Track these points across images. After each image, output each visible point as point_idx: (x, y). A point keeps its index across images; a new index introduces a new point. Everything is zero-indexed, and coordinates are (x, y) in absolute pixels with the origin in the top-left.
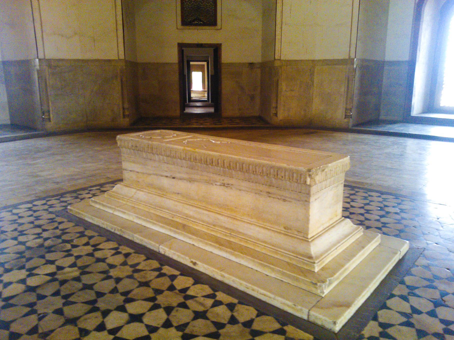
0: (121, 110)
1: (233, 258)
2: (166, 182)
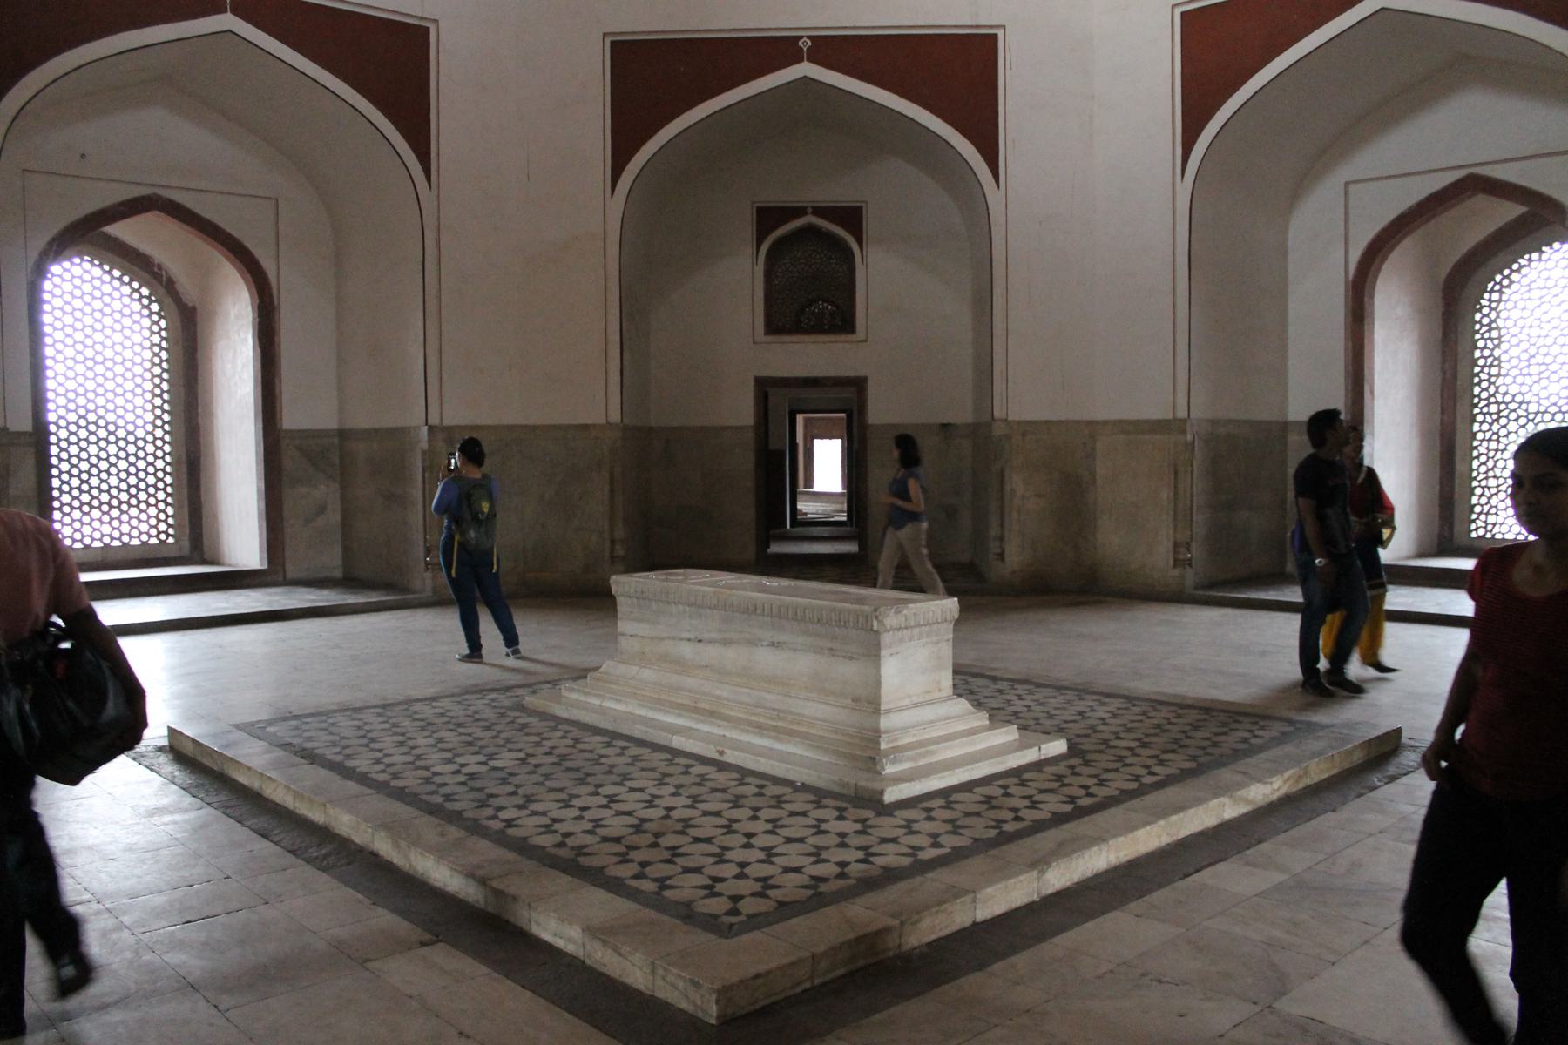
0: (608, 544)
1: (778, 746)
2: (687, 650)
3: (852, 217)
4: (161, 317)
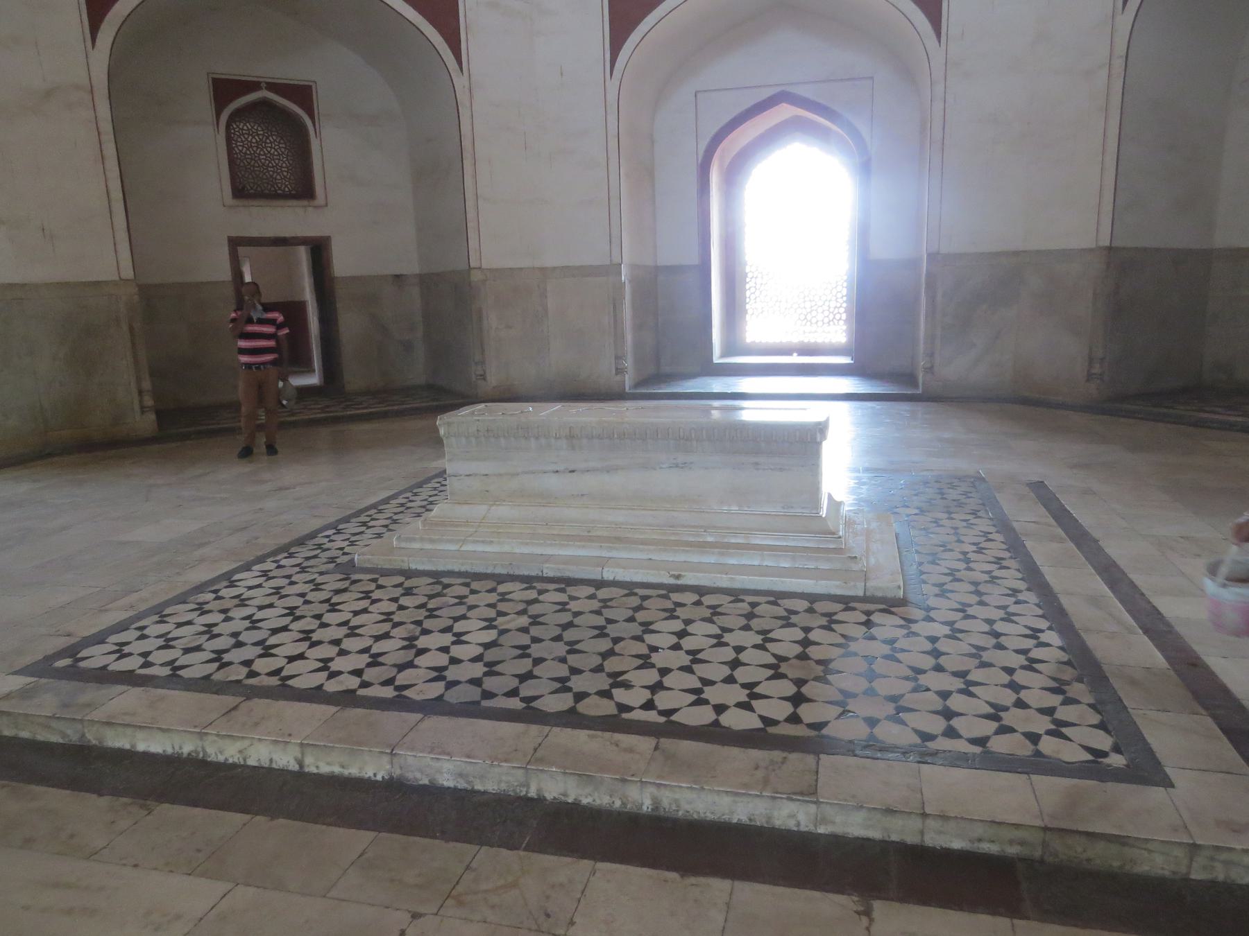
0: (136, 395)
2: (553, 483)
3: (302, 94)
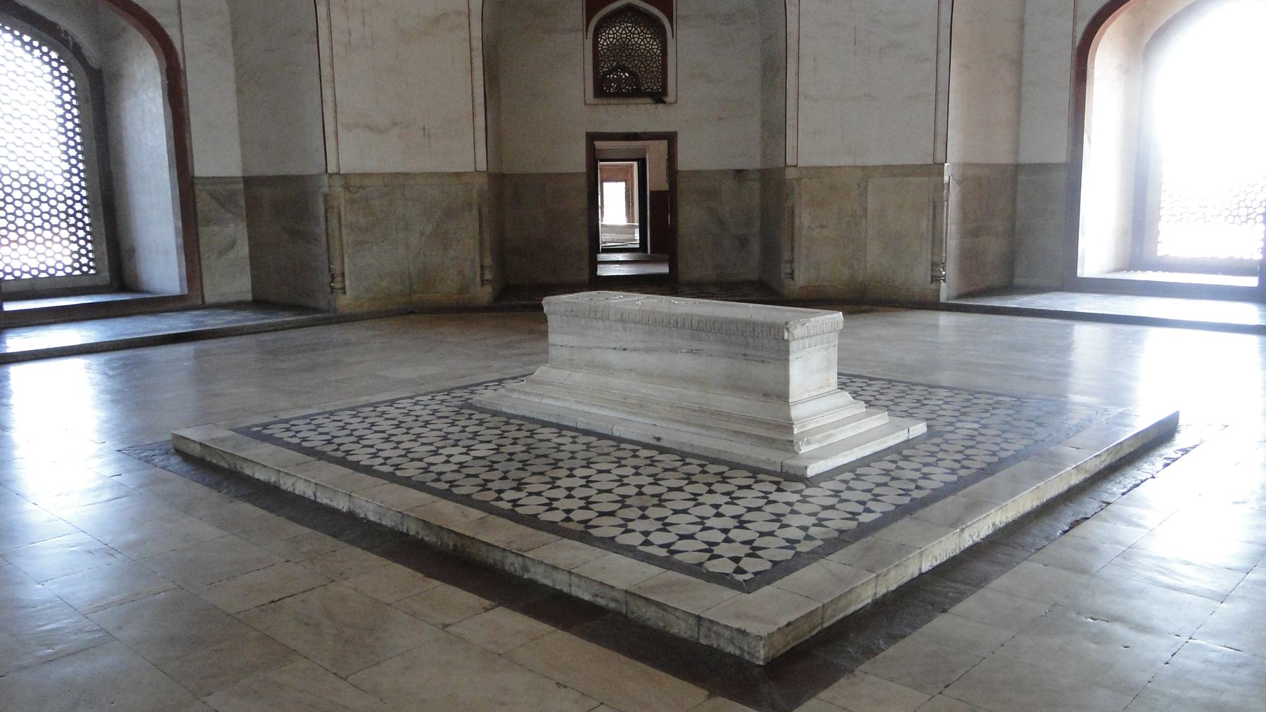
0: (478, 269)
2: (613, 357)
4: (70, 78)
